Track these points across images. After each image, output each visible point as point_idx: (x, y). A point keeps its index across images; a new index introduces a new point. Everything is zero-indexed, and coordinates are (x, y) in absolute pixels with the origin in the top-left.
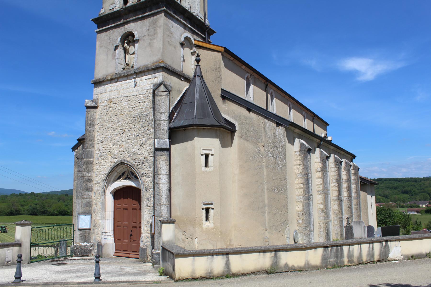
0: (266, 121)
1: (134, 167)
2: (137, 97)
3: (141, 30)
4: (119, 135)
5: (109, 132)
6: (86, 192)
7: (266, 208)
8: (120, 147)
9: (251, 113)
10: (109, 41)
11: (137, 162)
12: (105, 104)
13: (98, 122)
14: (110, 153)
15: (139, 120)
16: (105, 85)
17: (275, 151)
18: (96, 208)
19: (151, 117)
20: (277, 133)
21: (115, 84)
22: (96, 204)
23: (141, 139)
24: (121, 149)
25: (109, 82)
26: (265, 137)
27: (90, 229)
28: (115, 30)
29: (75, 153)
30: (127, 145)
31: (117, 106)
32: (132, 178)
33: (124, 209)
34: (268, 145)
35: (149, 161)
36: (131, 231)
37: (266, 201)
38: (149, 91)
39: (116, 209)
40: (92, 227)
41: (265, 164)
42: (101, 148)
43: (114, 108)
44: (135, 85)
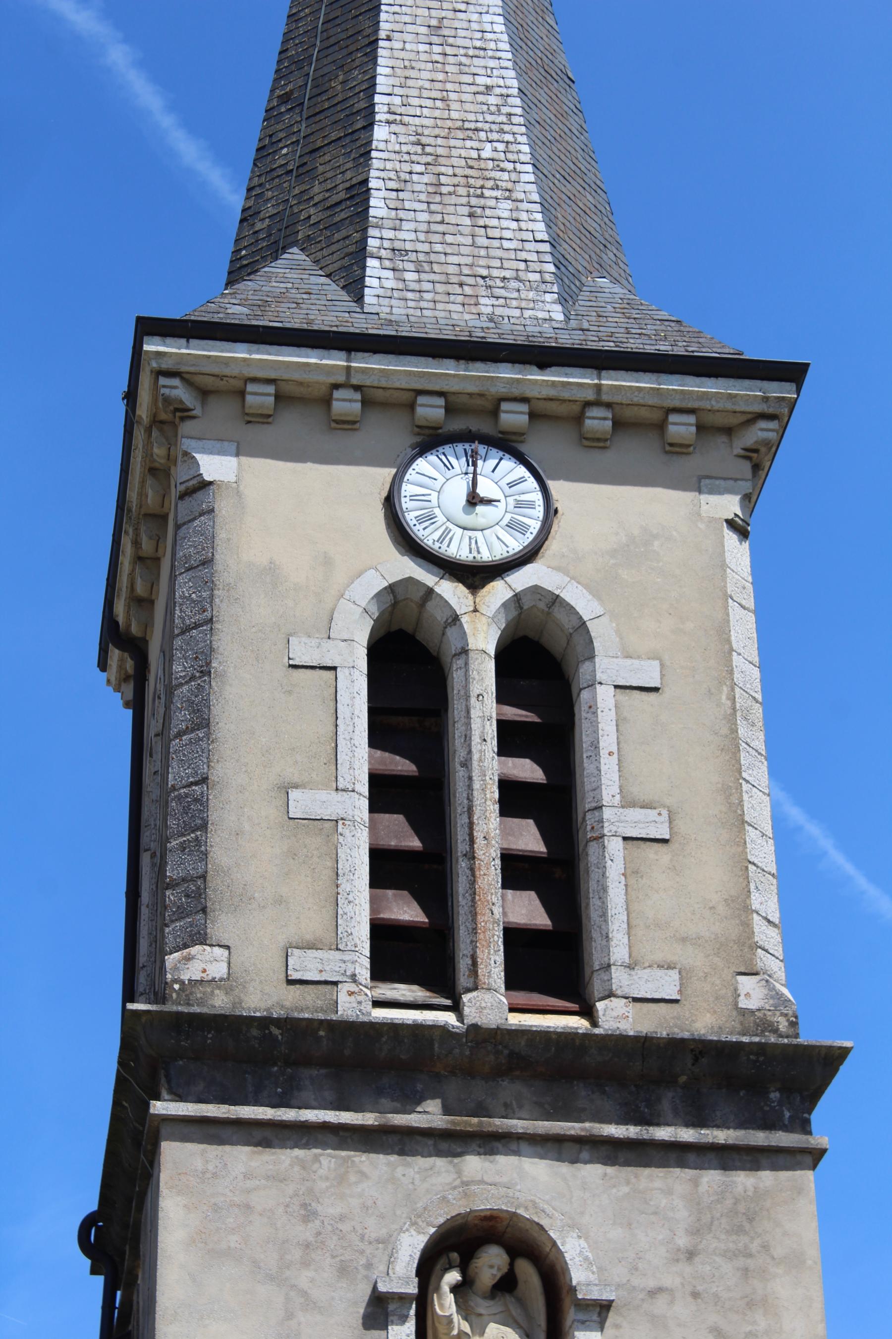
3: (617, 1233)
10: (306, 1233)
28: (364, 1161)
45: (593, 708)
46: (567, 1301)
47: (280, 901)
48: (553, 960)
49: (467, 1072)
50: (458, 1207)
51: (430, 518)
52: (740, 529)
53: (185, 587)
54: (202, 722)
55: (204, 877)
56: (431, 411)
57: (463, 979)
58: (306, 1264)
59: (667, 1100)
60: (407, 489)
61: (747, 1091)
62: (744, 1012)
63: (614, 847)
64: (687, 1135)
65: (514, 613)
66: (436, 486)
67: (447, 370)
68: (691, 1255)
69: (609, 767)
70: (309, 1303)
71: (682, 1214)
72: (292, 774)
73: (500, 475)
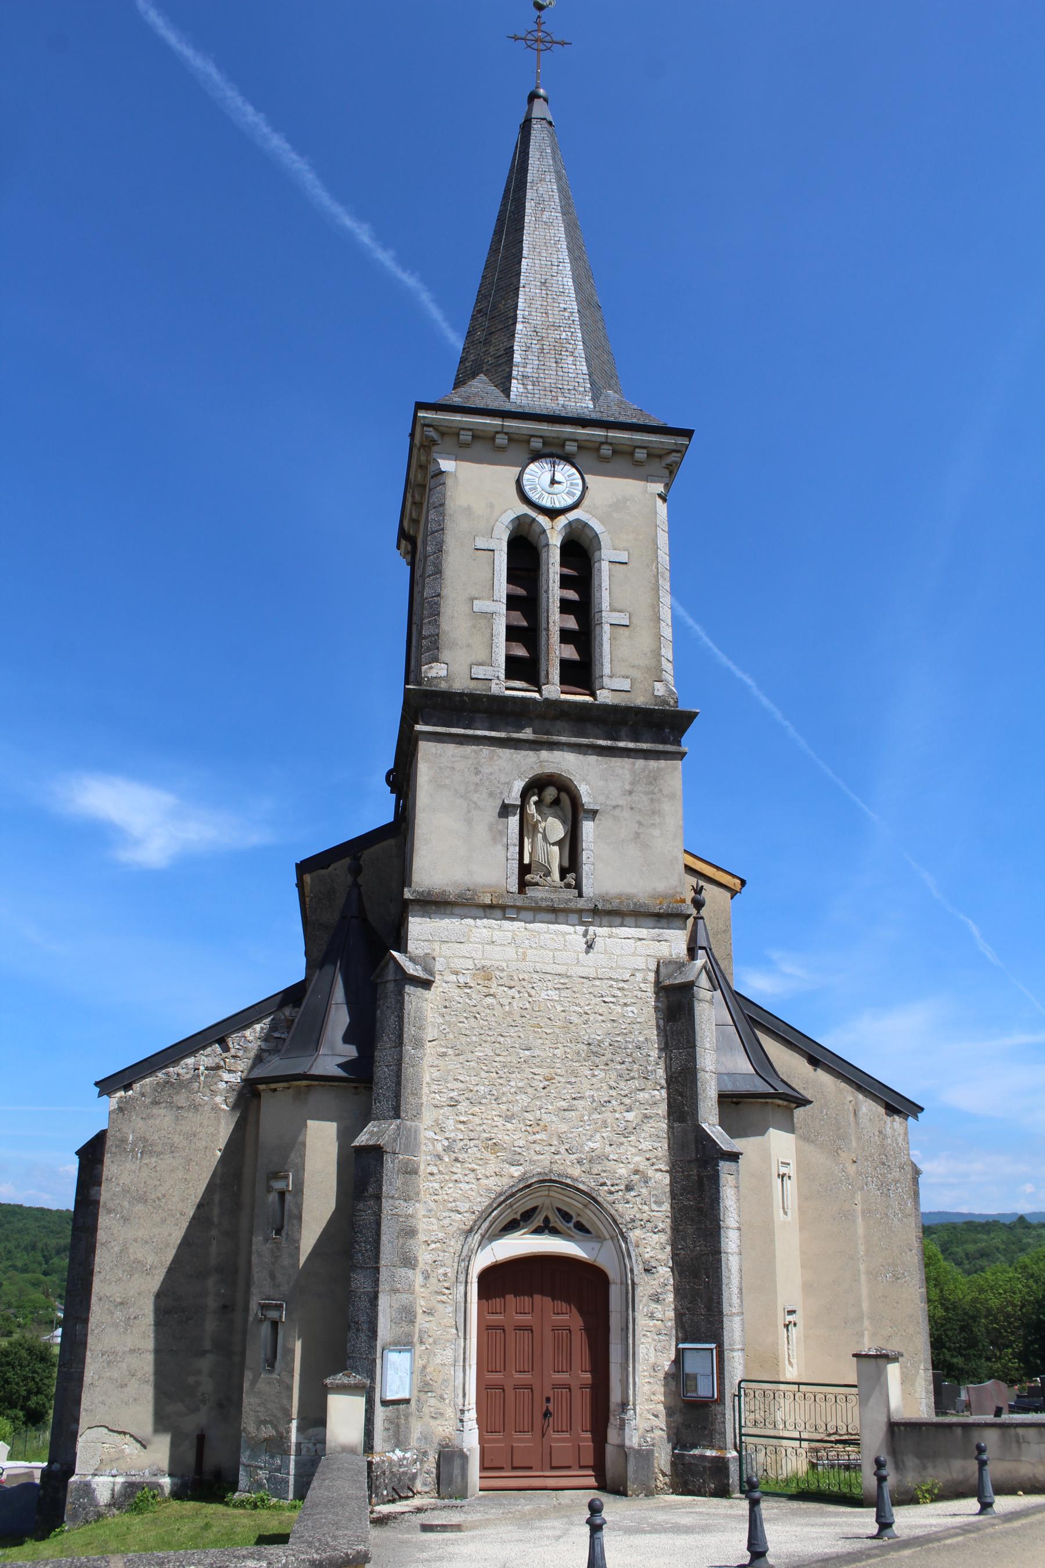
0: (861, 1097)
1: (599, 1199)
2: (597, 982)
3: (601, 783)
4: (530, 1090)
5: (483, 1074)
6: (403, 1271)
7: (866, 1323)
8: (537, 1129)
9: (819, 1070)
11: (609, 1183)
12: (462, 980)
13: (430, 1033)
14: (495, 1147)
15: (609, 1056)
16: (463, 917)
17: (884, 1175)
18: (433, 1326)
19: (651, 1053)
20: (889, 1131)
21: (506, 924)
22: (429, 1312)
23: (617, 1115)
24: (538, 1137)
25: (480, 912)
26: (859, 1139)
27: (407, 1401)
29: (112, 1102)
30: (563, 1127)
31: (517, 996)
32: (569, 1228)
33: (518, 1328)
34: (867, 1159)
35: (651, 1183)
36: (548, 1400)
37: (865, 1305)
38: (639, 976)
39: (486, 1329)
40: (415, 1392)
41: (859, 1208)
42: (450, 1124)
43: (504, 1001)
44: (590, 946)
45: (600, 570)
46: (580, 809)
47: (469, 646)
48: (580, 673)
49: (543, 717)
50: (538, 771)
51: (535, 489)
52: (663, 498)
53: (432, 515)
54: (439, 571)
55: (438, 635)
56: (537, 444)
57: (543, 680)
58: (476, 791)
59: (624, 731)
60: (526, 477)
61: (656, 728)
62: (656, 697)
63: (606, 628)
64: (631, 745)
65: (568, 530)
66: (538, 475)
67: (544, 427)
68: (630, 793)
69: (605, 595)
70: (477, 807)
71: (628, 776)
72: (475, 594)
73: (565, 472)
